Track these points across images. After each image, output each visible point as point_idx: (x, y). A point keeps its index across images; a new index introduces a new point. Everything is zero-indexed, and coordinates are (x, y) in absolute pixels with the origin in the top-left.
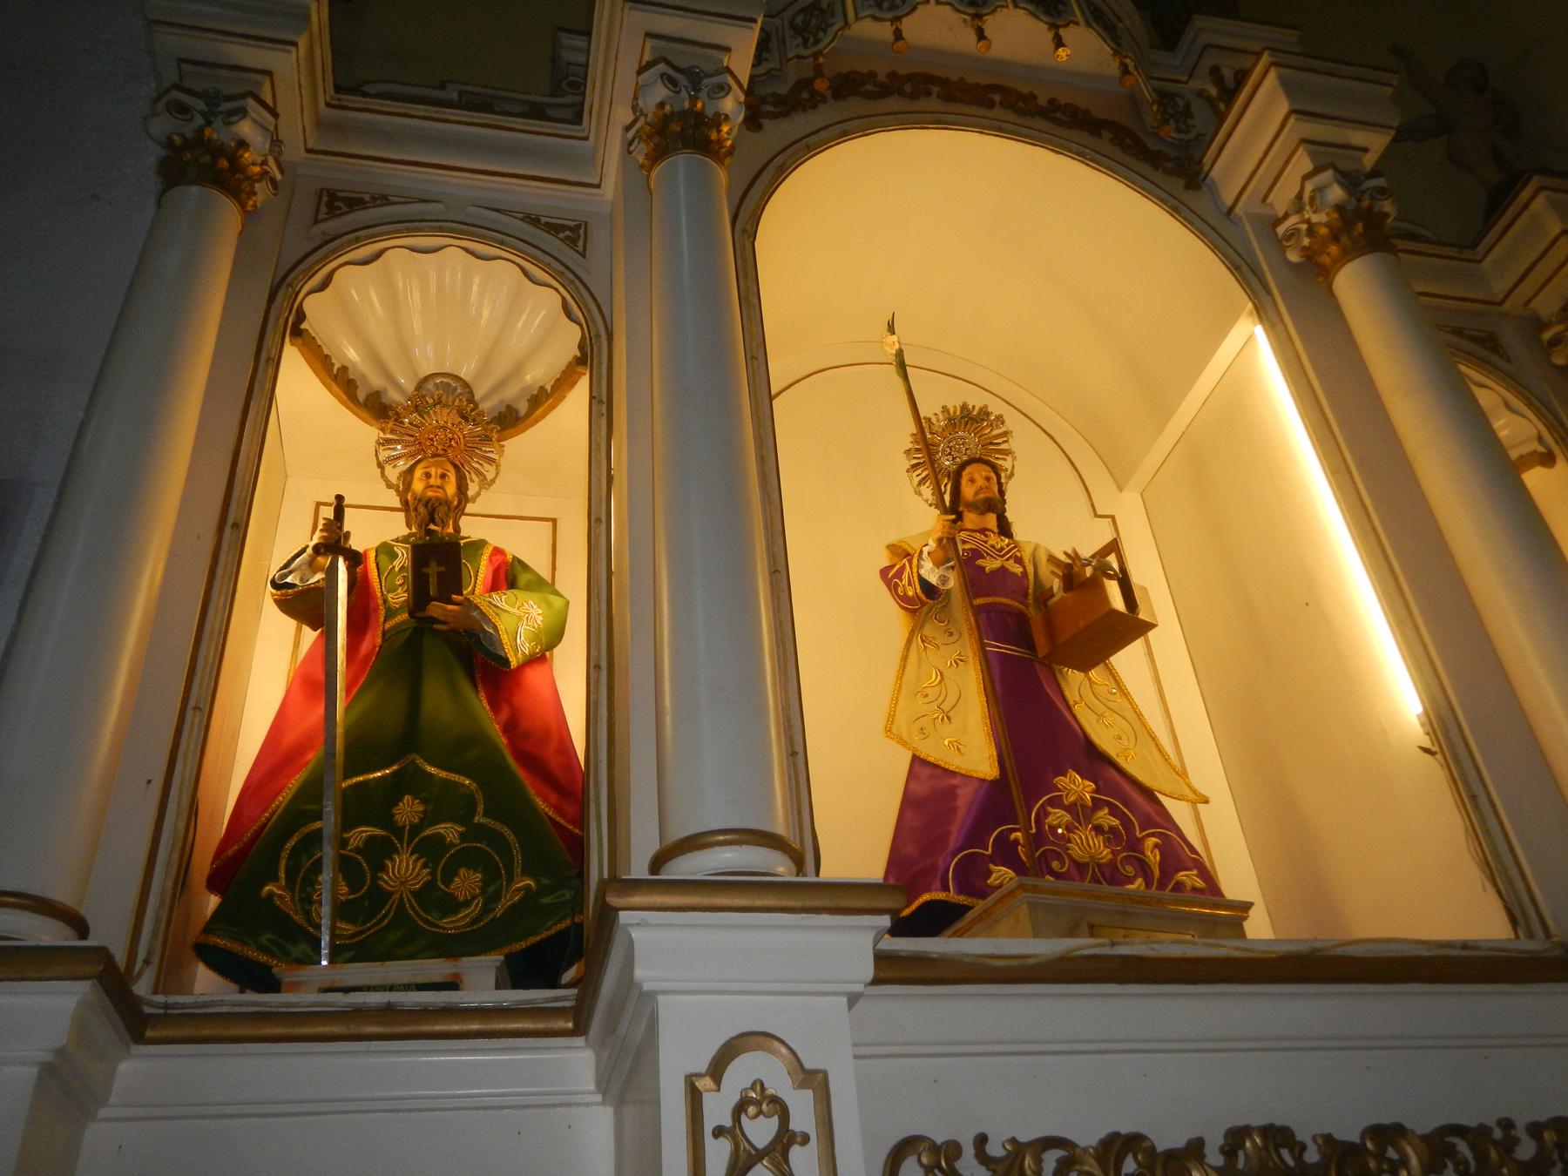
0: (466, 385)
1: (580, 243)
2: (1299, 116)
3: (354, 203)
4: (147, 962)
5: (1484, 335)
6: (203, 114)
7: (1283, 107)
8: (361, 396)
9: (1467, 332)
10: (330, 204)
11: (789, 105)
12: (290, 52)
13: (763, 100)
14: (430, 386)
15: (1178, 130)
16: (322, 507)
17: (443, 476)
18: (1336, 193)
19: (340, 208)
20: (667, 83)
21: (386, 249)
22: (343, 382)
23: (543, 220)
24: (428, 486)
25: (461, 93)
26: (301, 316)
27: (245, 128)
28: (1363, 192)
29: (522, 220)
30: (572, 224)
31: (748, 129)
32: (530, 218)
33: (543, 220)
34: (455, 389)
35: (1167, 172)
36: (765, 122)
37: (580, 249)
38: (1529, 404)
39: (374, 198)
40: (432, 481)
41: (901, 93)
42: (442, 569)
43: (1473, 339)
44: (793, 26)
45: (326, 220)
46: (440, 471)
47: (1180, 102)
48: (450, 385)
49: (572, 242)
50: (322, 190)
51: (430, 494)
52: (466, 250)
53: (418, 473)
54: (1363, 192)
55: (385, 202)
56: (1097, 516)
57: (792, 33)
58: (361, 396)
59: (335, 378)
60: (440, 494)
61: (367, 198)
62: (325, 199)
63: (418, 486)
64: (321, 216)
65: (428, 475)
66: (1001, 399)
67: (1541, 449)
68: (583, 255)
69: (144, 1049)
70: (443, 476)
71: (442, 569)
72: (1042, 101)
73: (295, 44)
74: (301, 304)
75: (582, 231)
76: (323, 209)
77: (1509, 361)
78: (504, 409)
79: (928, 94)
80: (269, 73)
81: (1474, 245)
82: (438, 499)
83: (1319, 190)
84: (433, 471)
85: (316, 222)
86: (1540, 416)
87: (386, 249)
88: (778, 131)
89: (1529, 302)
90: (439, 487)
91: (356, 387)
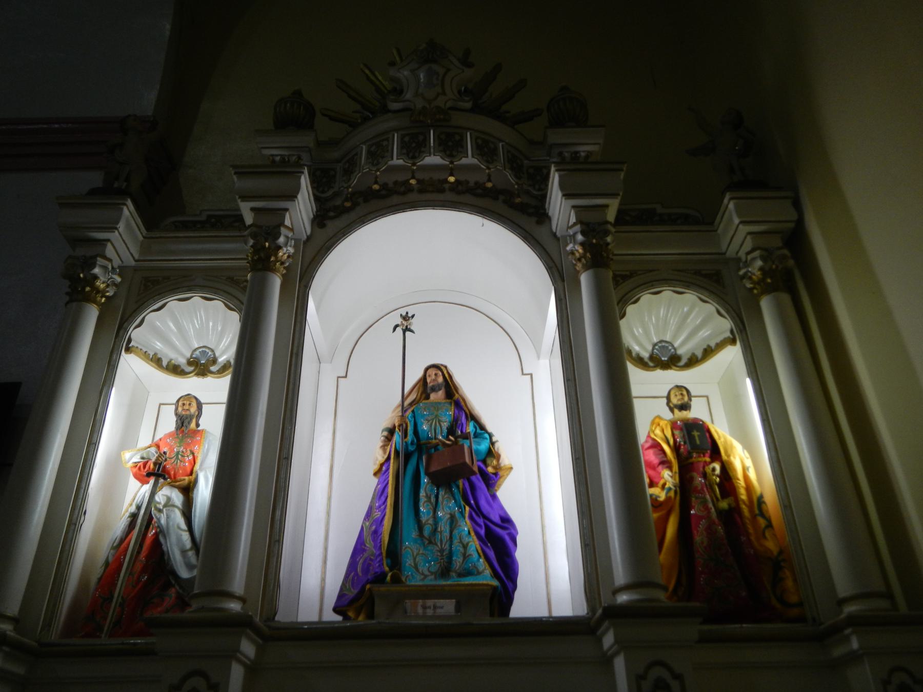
0: (212, 351)
2: (566, 197)
7: (560, 194)
8: (165, 363)
11: (341, 211)
12: (114, 232)
14: (197, 352)
16: (162, 406)
17: (190, 404)
18: (580, 237)
22: (156, 361)
24: (183, 410)
26: (130, 340)
27: (97, 271)
33: (235, 278)
34: (208, 353)
38: (728, 312)
40: (185, 407)
46: (188, 402)
48: (206, 351)
51: (184, 413)
52: (202, 297)
53: (180, 403)
56: (523, 374)
58: (165, 363)
59: (151, 360)
60: (188, 413)
63: (180, 409)
65: (184, 404)
66: (484, 314)
67: (731, 336)
70: (190, 404)
72: (472, 184)
73: (116, 228)
80: (108, 240)
81: (712, 223)
82: (187, 415)
83: (575, 234)
84: (185, 402)
86: (733, 318)
87: (167, 303)
88: (332, 226)
89: (737, 252)
90: (187, 410)
91: (162, 361)
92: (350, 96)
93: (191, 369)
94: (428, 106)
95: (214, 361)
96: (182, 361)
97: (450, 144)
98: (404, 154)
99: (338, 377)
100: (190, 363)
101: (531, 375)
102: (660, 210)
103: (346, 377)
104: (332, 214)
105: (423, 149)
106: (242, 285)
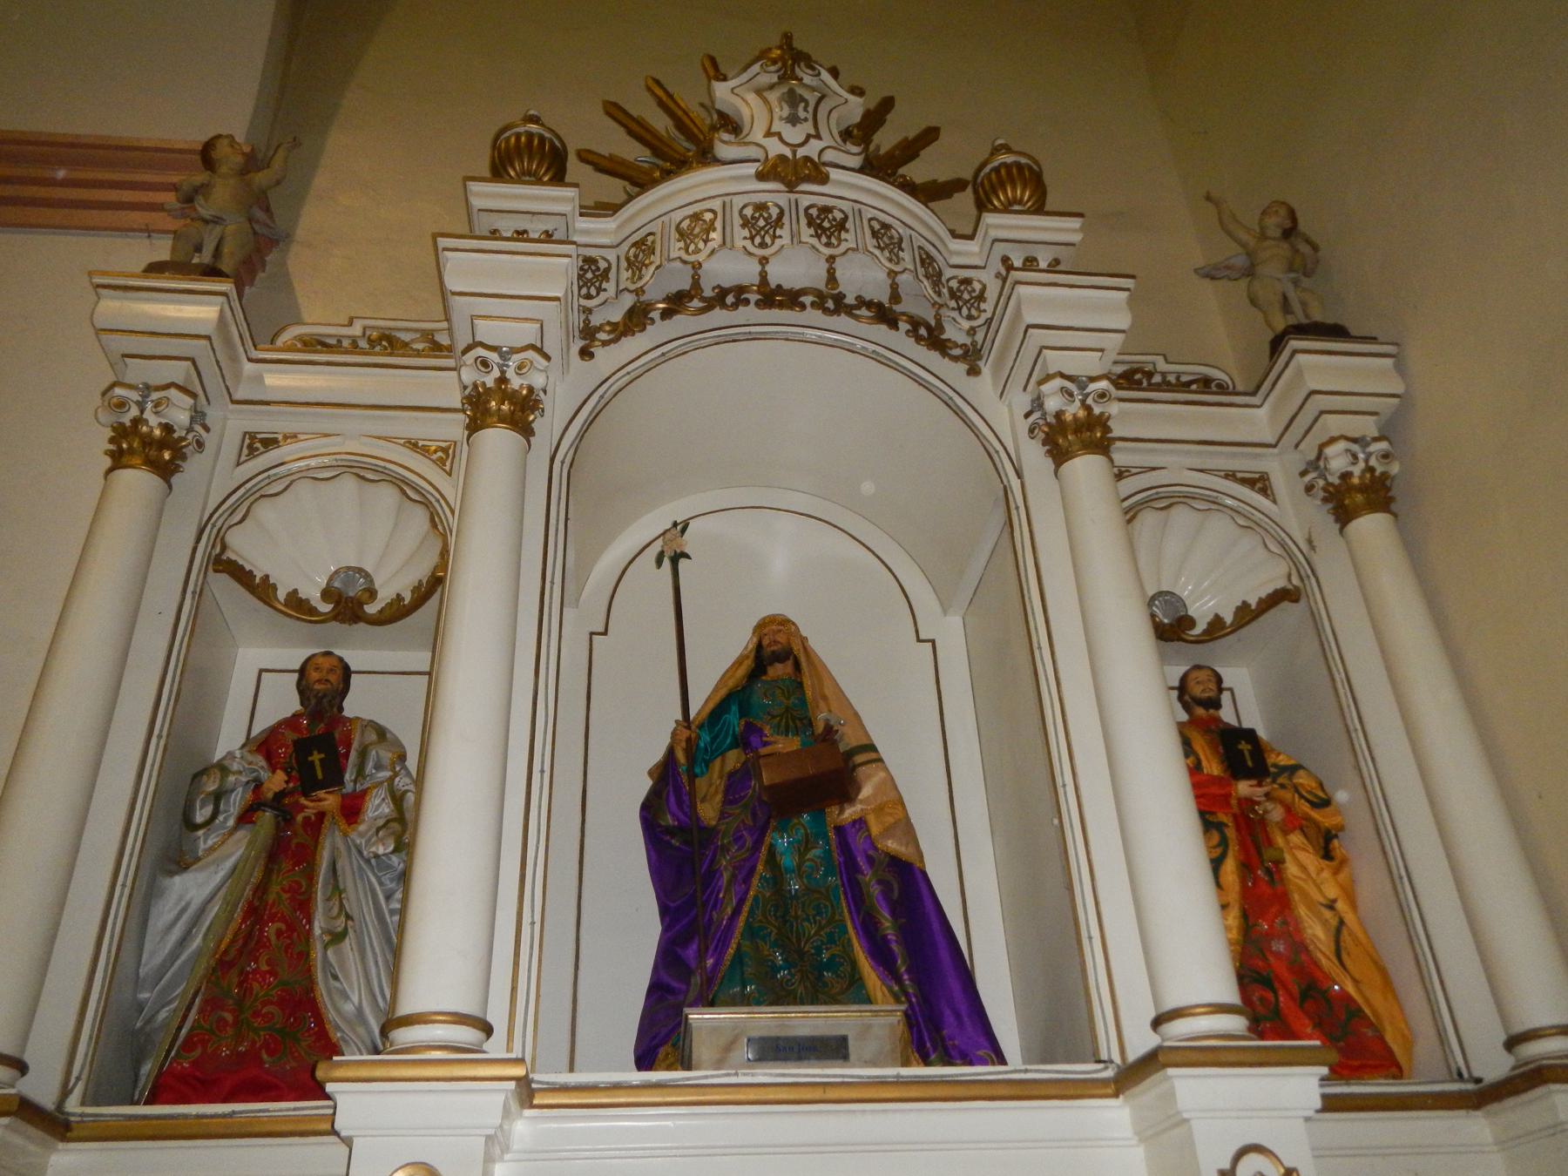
0: (367, 576)
1: (448, 463)
3: (270, 443)
4: (78, 1079)
5: (1257, 476)
6: (138, 403)
9: (1239, 475)
10: (250, 447)
13: (599, 329)
15: (970, 317)
19: (257, 449)
20: (480, 367)
21: (294, 481)
23: (421, 443)
25: (365, 329)
28: (1089, 394)
29: (403, 445)
30: (444, 445)
31: (583, 359)
32: (410, 443)
33: (421, 443)
35: (955, 359)
36: (599, 351)
37: (448, 468)
39: (286, 437)
41: (724, 305)
42: (322, 756)
43: (1244, 481)
44: (628, 259)
45: (246, 461)
47: (977, 286)
49: (441, 463)
50: (246, 433)
54: (1089, 394)
55: (295, 440)
56: (919, 640)
57: (626, 264)
58: (282, 595)
61: (280, 437)
62: (247, 441)
64: (243, 458)
68: (450, 474)
69: (72, 1145)
71: (322, 756)
74: (223, 539)
75: (451, 451)
76: (245, 451)
77: (1275, 502)
78: (395, 596)
79: (747, 302)
85: (238, 464)
92: (630, 133)
93: (326, 608)
94: (789, 155)
95: (372, 593)
96: (312, 592)
97: (826, 224)
98: (745, 238)
99: (592, 634)
100: (327, 594)
101: (933, 642)
102: (1162, 366)
103: (605, 633)
104: (602, 336)
105: (778, 232)
106: (434, 457)
